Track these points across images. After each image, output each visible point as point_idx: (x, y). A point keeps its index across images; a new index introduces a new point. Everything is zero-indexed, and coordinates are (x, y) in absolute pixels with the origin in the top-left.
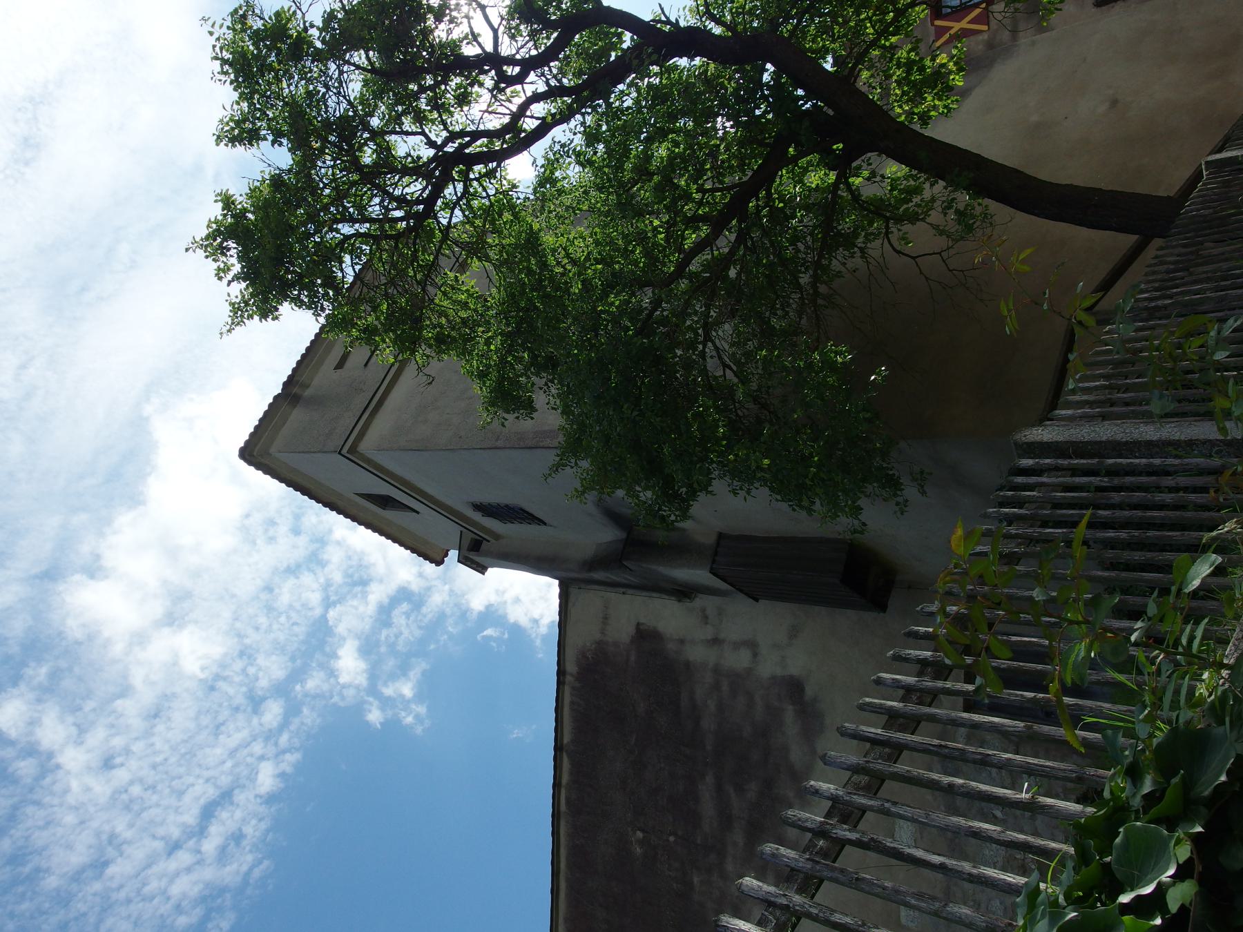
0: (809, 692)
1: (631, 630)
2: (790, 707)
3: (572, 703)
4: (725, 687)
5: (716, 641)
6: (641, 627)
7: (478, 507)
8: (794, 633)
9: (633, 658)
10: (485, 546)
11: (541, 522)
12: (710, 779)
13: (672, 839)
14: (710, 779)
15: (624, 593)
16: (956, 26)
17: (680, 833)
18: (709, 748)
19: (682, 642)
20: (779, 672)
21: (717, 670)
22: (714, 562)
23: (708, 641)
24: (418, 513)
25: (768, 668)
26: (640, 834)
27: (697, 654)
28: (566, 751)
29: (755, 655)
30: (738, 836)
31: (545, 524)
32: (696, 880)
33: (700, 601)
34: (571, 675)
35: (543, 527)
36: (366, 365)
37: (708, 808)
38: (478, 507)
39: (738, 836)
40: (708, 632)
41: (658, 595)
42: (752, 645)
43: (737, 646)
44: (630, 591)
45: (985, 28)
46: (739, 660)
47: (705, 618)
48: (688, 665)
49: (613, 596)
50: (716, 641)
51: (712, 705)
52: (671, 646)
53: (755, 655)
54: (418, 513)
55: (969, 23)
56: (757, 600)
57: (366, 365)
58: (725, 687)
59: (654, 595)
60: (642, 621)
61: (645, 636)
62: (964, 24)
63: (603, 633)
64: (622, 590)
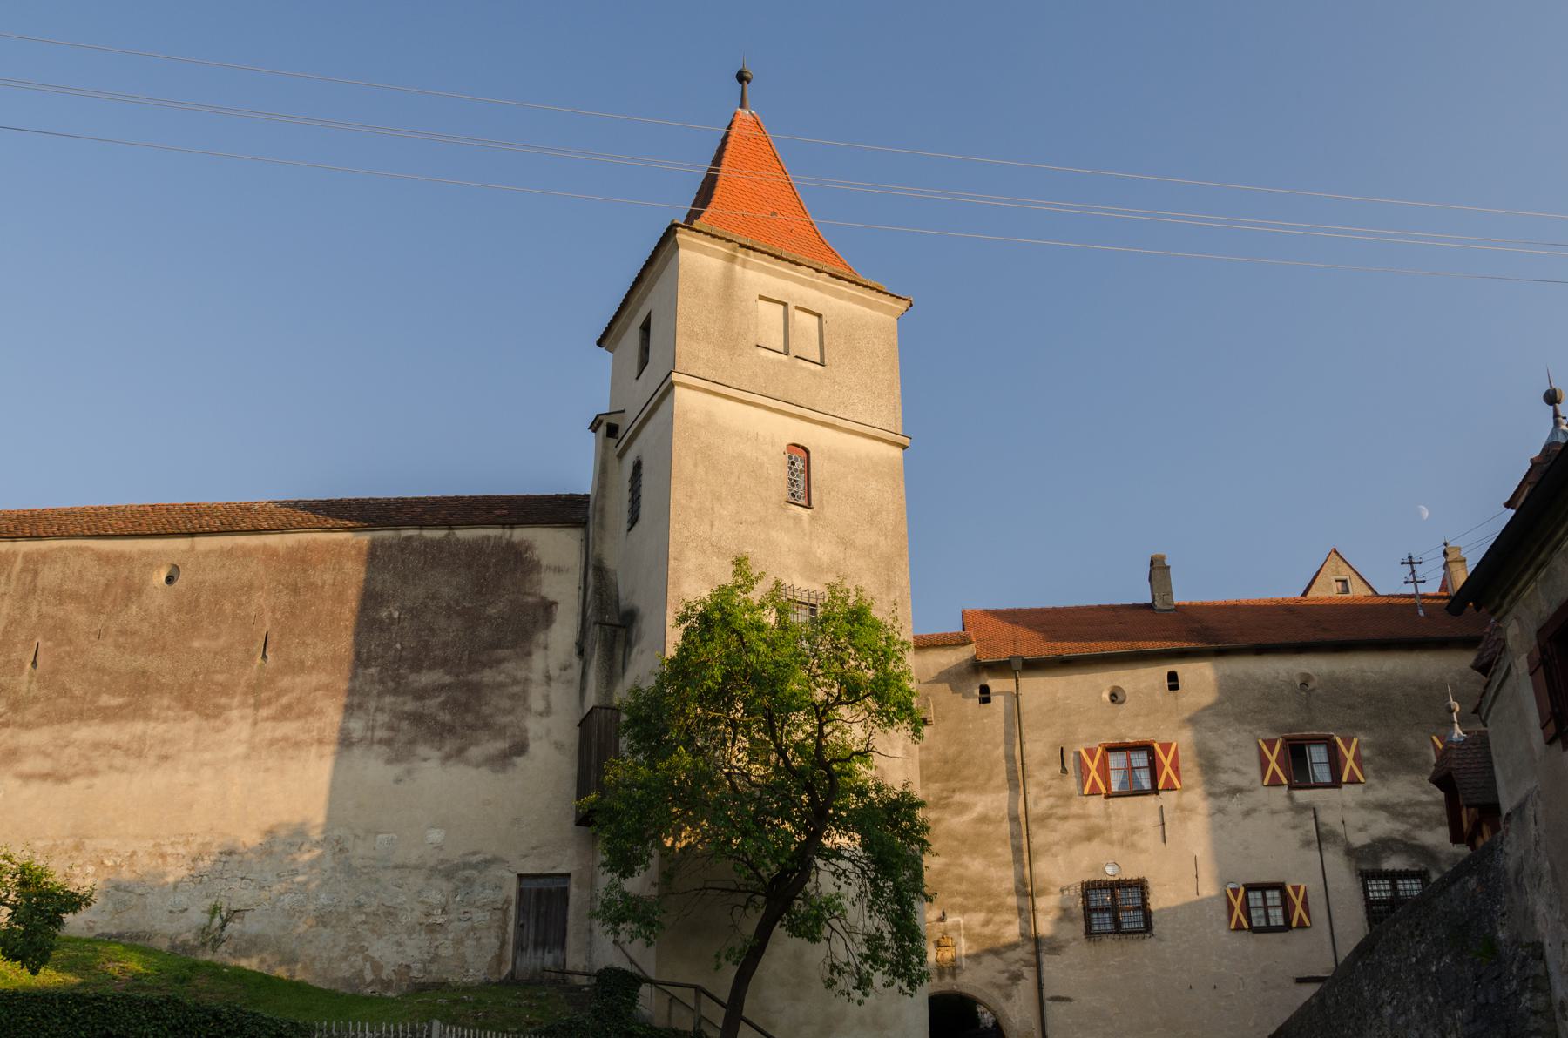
0: (518, 760)
1: (551, 597)
2: (507, 746)
3: (488, 538)
4: (516, 689)
5: (548, 679)
6: (554, 607)
7: (638, 466)
8: (559, 746)
9: (530, 599)
10: (613, 441)
11: (630, 530)
12: (448, 679)
13: (398, 646)
14: (448, 679)
15: (580, 588)
16: (1093, 767)
17: (404, 653)
18: (470, 677)
19: (546, 648)
20: (530, 735)
21: (527, 681)
22: (601, 708)
23: (548, 672)
24: (637, 378)
25: (534, 726)
26: (396, 615)
27: (538, 661)
28: (449, 534)
29: (541, 714)
30: (410, 706)
31: (630, 530)
32: (372, 670)
33: (576, 661)
34: (511, 536)
35: (626, 526)
36: (758, 346)
37: (426, 678)
38: (638, 466)
39: (410, 706)
40: (554, 672)
41: (580, 622)
42: (547, 712)
43: (546, 698)
44: (581, 593)
45: (1086, 792)
46: (537, 703)
47: (565, 668)
48: (529, 654)
49: (577, 576)
50: (548, 679)
51: (501, 678)
52: (541, 637)
53: (541, 714)
54: (637, 378)
55: (1094, 779)
56: (579, 725)
57: (758, 346)
58: (516, 689)
59: (580, 618)
60: (559, 607)
61: (547, 609)
62: (1094, 774)
63: (548, 567)
64: (582, 586)
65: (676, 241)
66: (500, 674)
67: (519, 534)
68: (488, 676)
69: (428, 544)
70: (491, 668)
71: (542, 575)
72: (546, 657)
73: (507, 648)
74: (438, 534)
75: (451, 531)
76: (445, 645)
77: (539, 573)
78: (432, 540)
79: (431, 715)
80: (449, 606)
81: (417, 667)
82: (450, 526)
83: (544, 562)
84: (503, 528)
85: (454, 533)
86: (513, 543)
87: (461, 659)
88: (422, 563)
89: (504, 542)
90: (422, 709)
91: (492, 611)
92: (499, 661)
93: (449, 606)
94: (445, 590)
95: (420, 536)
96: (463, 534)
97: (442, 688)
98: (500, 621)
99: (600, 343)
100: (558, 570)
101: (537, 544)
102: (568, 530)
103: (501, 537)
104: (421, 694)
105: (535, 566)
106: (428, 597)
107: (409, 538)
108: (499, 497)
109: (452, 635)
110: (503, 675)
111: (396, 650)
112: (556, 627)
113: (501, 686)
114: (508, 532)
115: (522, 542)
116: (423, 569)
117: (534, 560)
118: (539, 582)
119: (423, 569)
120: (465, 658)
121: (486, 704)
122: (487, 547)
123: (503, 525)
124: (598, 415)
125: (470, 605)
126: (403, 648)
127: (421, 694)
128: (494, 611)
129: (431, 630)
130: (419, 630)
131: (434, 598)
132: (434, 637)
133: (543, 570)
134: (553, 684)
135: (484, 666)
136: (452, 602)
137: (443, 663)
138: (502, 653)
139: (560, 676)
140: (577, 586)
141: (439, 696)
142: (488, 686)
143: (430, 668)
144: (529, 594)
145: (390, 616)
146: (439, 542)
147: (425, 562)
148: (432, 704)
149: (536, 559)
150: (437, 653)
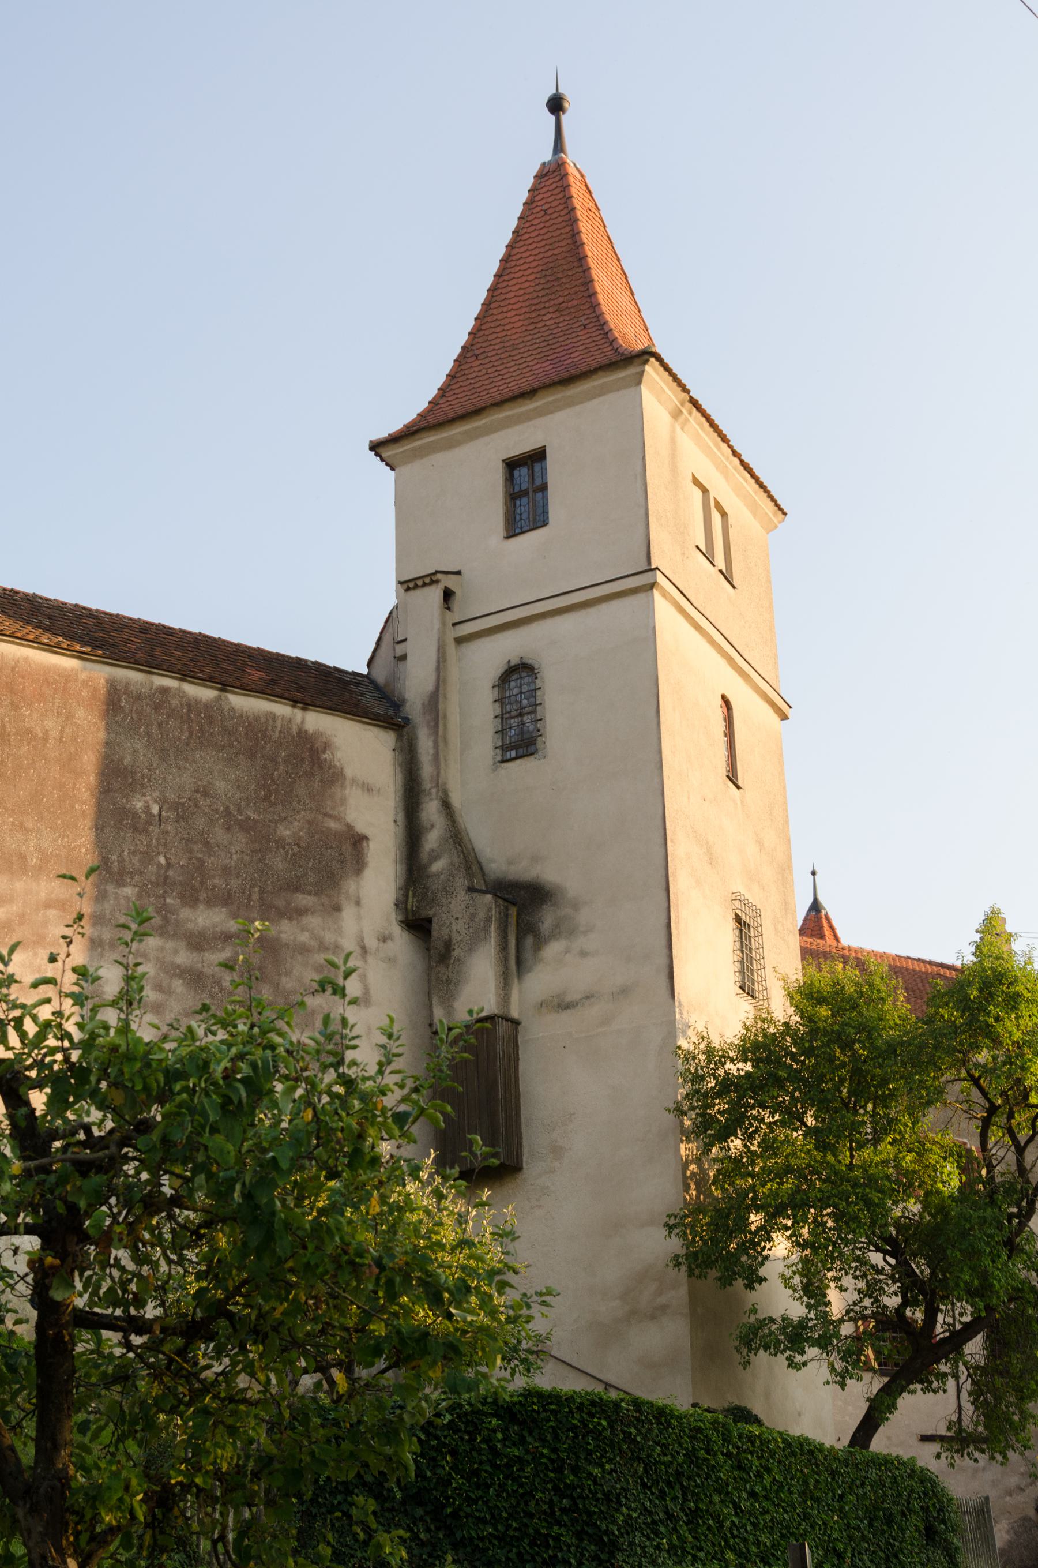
1: (361, 828)
3: (273, 717)
6: (365, 844)
9: (333, 825)
13: (162, 860)
17: (170, 873)
19: (358, 903)
23: (362, 940)
26: (155, 809)
28: (219, 698)
30: (184, 958)
32: (129, 891)
39: (184, 958)
40: (371, 943)
48: (338, 908)
51: (304, 938)
52: (350, 885)
60: (372, 844)
63: (354, 781)
65: (641, 373)
66: (302, 930)
67: (316, 721)
68: (287, 931)
69: (193, 705)
70: (290, 919)
71: (347, 792)
72: (359, 918)
73: (309, 893)
74: (205, 694)
75: (223, 694)
76: (226, 871)
77: (343, 786)
78: (197, 701)
79: (213, 976)
80: (228, 812)
81: (191, 899)
82: (224, 687)
83: (349, 772)
84: (294, 707)
85: (227, 699)
86: (306, 731)
87: (249, 897)
88: (187, 734)
89: (294, 730)
90: (200, 965)
91: (285, 832)
92: (301, 912)
93: (228, 812)
94: (221, 786)
95: (179, 689)
96: (241, 702)
97: (227, 937)
98: (296, 849)
99: (376, 447)
100: (368, 789)
101: (338, 741)
102: (376, 730)
103: (290, 721)
104: (198, 942)
105: (333, 777)
106: (197, 791)
107: (165, 691)
108: (239, 645)
109: (234, 856)
110: (307, 934)
111: (159, 865)
112: (368, 873)
113: (304, 950)
114: (298, 714)
115: (318, 734)
116: (188, 744)
117: (335, 767)
118: (343, 801)
119: (188, 744)
120: (255, 897)
121: (286, 974)
122: (274, 731)
123: (295, 702)
124: (437, 572)
125: (256, 817)
126: (169, 865)
127: (198, 942)
128: (288, 832)
129: (207, 844)
130: (188, 840)
131: (206, 794)
132: (210, 856)
133: (347, 783)
134: (370, 959)
135: (282, 914)
136: (232, 807)
137: (226, 899)
138: (303, 900)
139: (378, 949)
140: (391, 818)
141: (223, 949)
142: (287, 946)
143: (210, 903)
144: (331, 816)
145: (147, 809)
146: (207, 706)
147: (191, 734)
148: (212, 959)
149: (338, 764)
150: (216, 881)
